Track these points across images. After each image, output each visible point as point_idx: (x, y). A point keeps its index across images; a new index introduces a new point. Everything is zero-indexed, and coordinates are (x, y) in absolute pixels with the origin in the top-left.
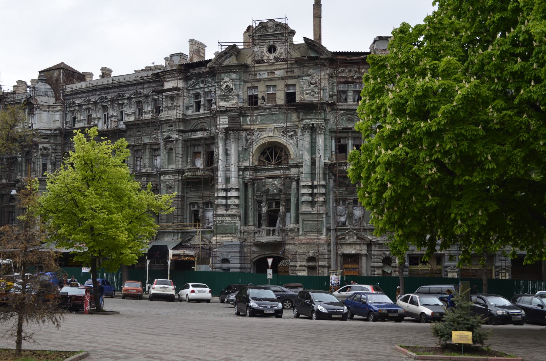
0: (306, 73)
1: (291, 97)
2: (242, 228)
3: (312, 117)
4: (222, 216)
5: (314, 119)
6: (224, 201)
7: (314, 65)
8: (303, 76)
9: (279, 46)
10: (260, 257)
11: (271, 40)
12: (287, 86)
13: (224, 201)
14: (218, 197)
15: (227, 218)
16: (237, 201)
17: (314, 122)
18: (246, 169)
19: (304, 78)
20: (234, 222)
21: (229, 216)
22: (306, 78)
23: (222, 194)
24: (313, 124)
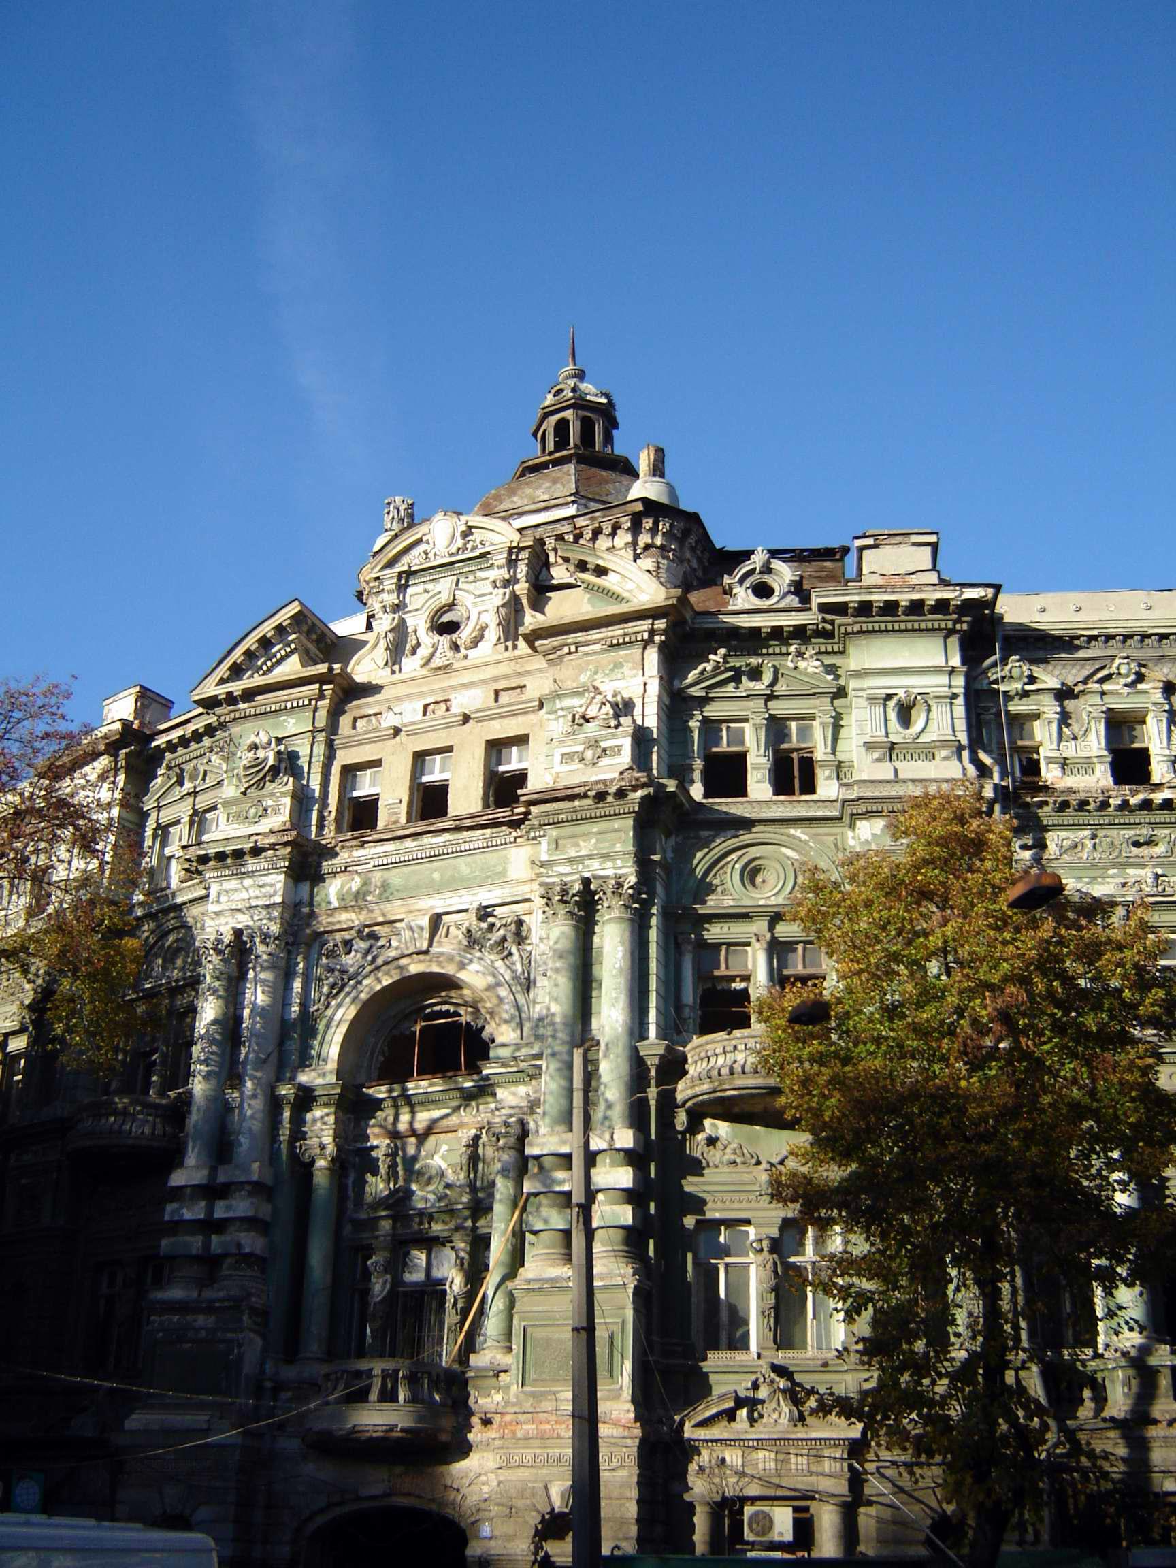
0: (570, 684)
2: (269, 1367)
3: (583, 852)
4: (182, 1307)
5: (590, 857)
6: (195, 1243)
7: (602, 651)
8: (556, 696)
10: (337, 1511)
11: (443, 588)
12: (496, 747)
13: (195, 1243)
14: (178, 1226)
15: (201, 1320)
16: (251, 1242)
17: (593, 868)
19: (558, 705)
20: (229, 1335)
21: (209, 1309)
22: (568, 702)
23: (193, 1212)
24: (586, 882)
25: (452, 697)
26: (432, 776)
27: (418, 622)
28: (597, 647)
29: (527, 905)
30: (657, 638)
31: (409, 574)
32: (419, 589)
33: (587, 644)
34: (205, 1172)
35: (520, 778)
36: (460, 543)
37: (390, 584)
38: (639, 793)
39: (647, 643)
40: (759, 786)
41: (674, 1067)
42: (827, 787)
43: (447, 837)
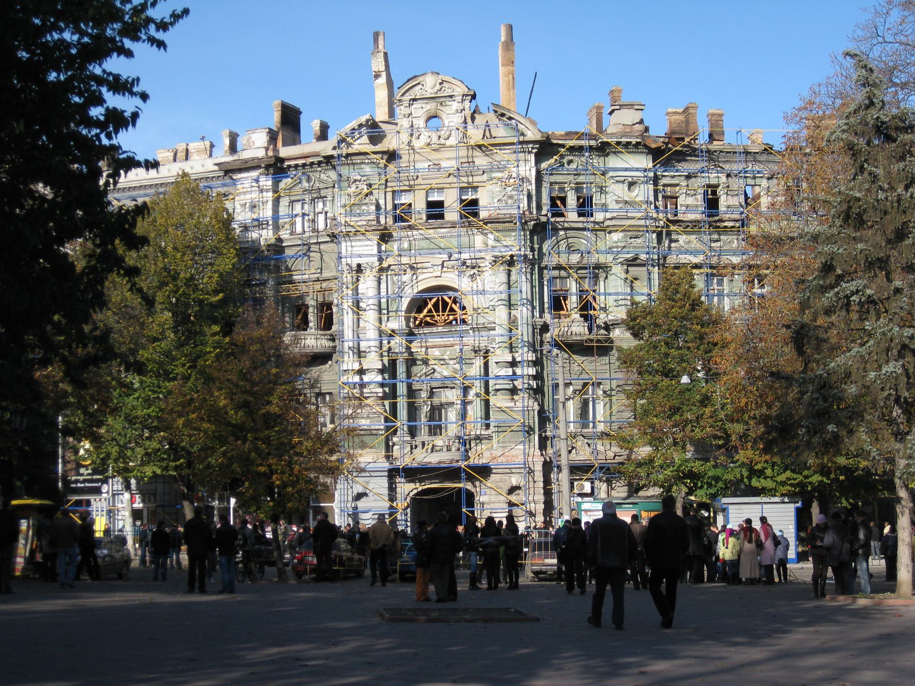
1: (471, 207)
7: (511, 153)
9: (447, 118)
18: (393, 334)
25: (441, 163)
26: (435, 197)
27: (420, 123)
28: (509, 151)
29: (482, 260)
30: (535, 151)
31: (415, 100)
32: (420, 106)
33: (504, 149)
34: (358, 364)
35: (475, 202)
36: (438, 87)
37: (406, 103)
38: (533, 222)
39: (530, 152)
40: (572, 216)
41: (545, 328)
42: (599, 216)
43: (448, 229)
